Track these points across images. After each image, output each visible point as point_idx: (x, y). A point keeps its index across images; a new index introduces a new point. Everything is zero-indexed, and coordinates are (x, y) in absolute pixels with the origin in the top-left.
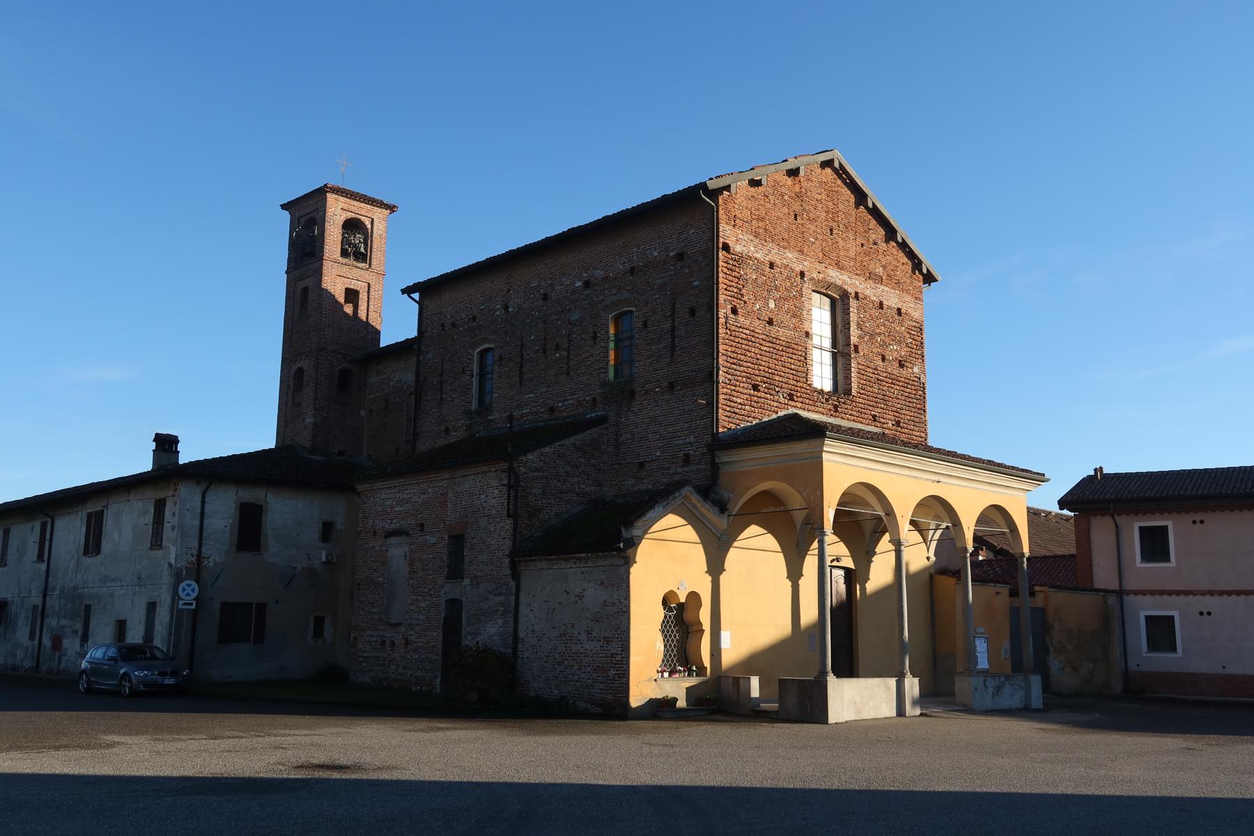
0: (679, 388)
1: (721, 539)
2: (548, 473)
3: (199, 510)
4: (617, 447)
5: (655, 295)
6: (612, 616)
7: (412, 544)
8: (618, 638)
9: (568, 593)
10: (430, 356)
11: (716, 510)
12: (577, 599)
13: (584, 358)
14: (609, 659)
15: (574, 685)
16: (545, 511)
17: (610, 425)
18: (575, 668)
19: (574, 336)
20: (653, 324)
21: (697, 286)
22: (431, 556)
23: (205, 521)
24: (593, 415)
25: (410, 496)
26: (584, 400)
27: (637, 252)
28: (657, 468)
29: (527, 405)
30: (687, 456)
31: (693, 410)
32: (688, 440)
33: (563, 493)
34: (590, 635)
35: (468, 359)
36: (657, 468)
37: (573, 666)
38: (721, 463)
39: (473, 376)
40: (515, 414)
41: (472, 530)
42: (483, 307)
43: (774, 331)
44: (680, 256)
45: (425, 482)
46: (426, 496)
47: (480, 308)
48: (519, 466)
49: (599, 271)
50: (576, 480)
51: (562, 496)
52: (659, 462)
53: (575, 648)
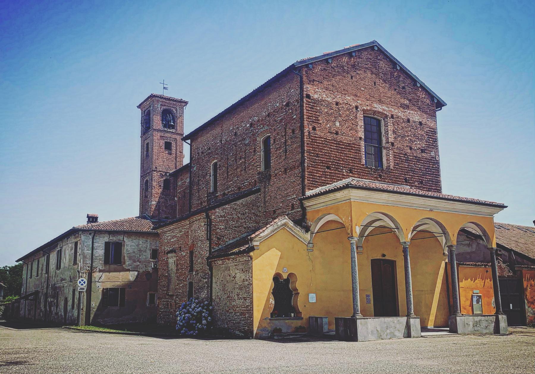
0: (289, 171)
1: (308, 246)
2: (228, 218)
3: (91, 246)
4: (265, 203)
5: (278, 126)
6: (246, 286)
7: (177, 257)
8: (249, 297)
9: (230, 276)
10: (195, 169)
11: (303, 230)
12: (233, 279)
13: (251, 162)
14: (246, 308)
15: (233, 322)
16: (226, 237)
17: (262, 193)
18: (233, 314)
19: (247, 151)
20: (278, 140)
21: (295, 118)
22: (183, 262)
23: (94, 251)
24: (255, 189)
25: (176, 234)
26: (252, 182)
27: (270, 105)
28: (281, 212)
29: (230, 187)
30: (293, 205)
31: (295, 181)
32: (293, 197)
33: (237, 227)
34: (239, 297)
35: (208, 168)
36: (281, 212)
37: (232, 313)
38: (306, 207)
39: (211, 176)
40: (226, 192)
41: (195, 248)
42: (213, 142)
43: (339, 138)
44: (288, 105)
45: (181, 227)
46: (182, 233)
47: (212, 143)
48: (211, 215)
49: (256, 118)
50: (243, 220)
51: (236, 229)
52: (282, 209)
53: (234, 303)
